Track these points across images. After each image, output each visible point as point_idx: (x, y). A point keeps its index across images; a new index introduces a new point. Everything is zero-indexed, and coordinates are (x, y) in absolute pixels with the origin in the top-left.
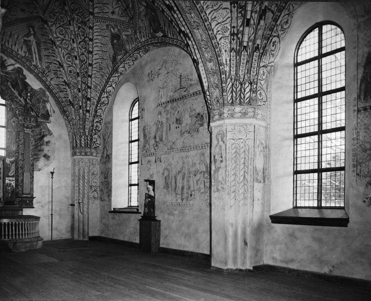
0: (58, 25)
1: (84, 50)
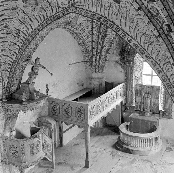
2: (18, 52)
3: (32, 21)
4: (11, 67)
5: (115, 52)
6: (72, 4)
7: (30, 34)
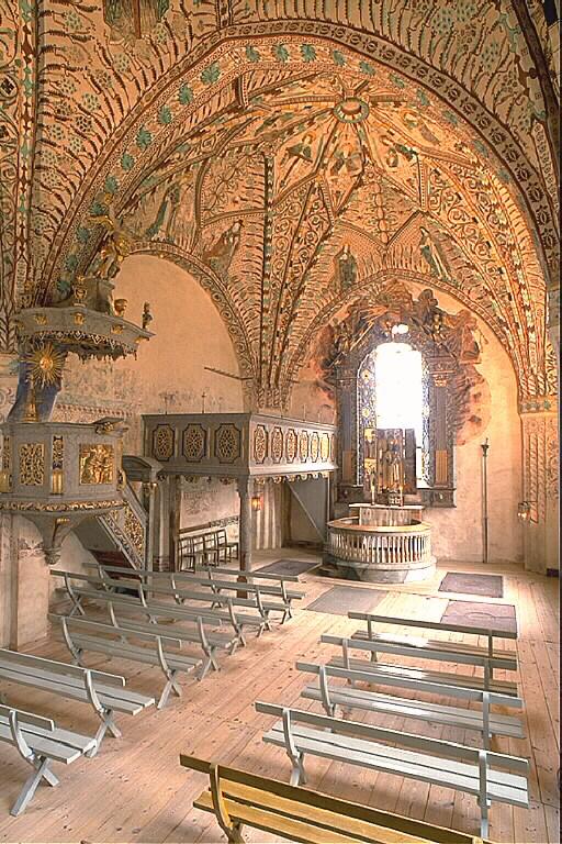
0: (448, 208)
1: (497, 226)
2: (81, 183)
3: (124, 87)
4: (56, 226)
5: (312, 362)
6: (225, 22)
7: (116, 128)
